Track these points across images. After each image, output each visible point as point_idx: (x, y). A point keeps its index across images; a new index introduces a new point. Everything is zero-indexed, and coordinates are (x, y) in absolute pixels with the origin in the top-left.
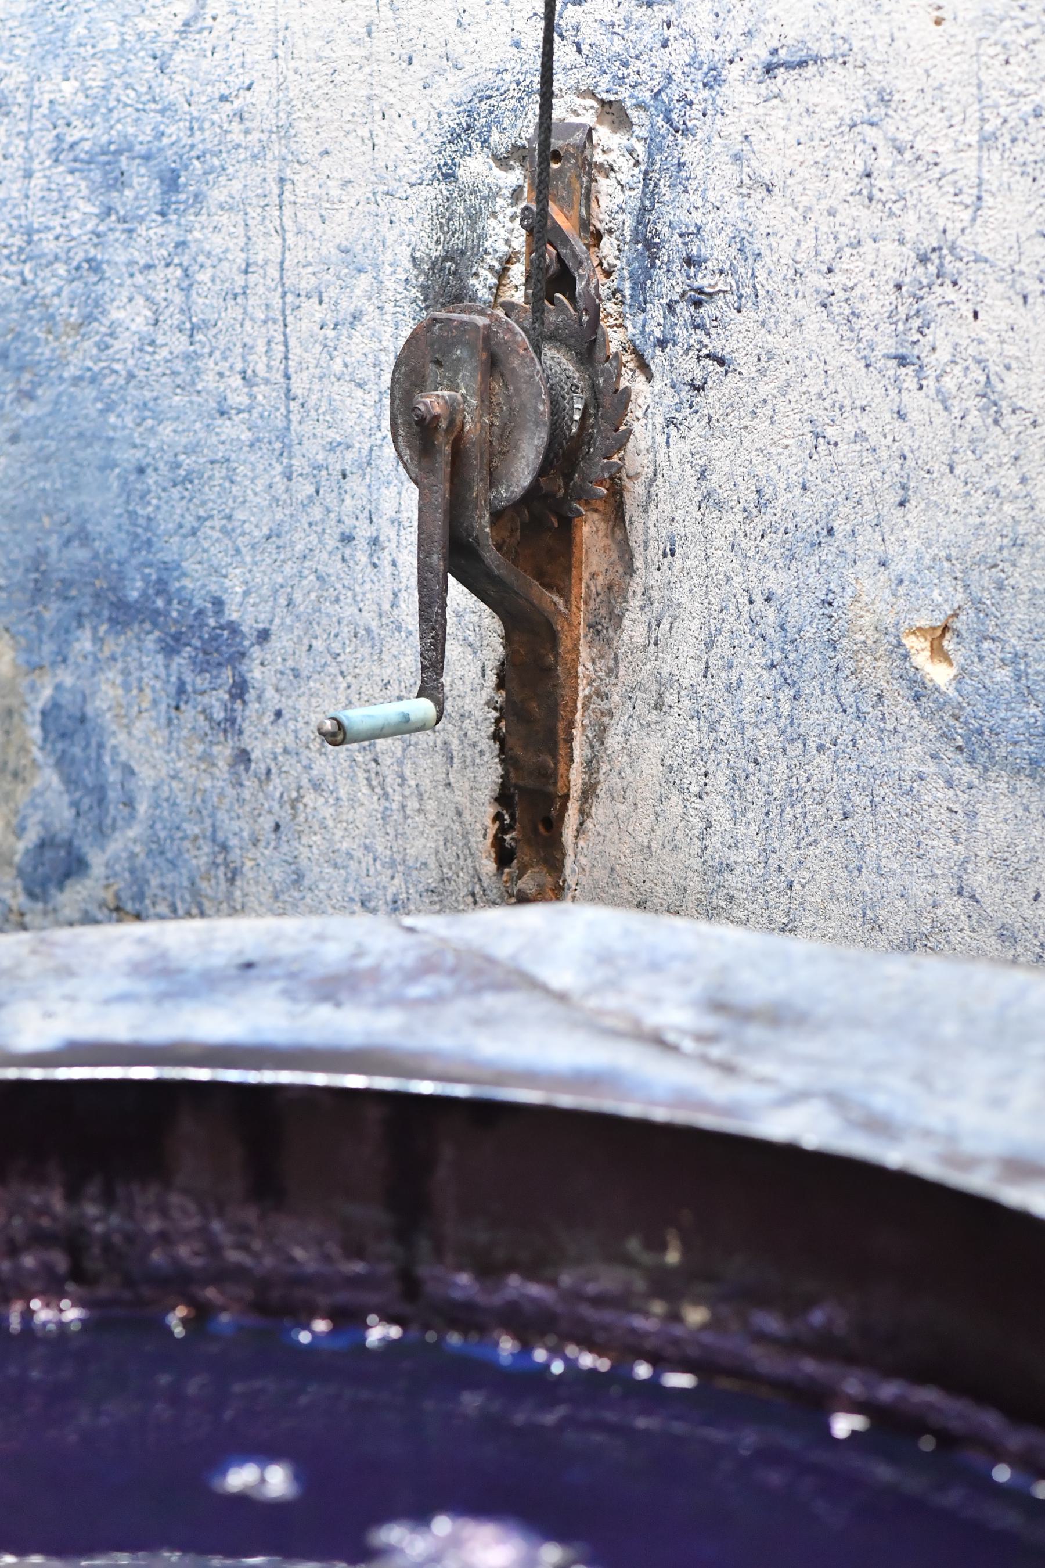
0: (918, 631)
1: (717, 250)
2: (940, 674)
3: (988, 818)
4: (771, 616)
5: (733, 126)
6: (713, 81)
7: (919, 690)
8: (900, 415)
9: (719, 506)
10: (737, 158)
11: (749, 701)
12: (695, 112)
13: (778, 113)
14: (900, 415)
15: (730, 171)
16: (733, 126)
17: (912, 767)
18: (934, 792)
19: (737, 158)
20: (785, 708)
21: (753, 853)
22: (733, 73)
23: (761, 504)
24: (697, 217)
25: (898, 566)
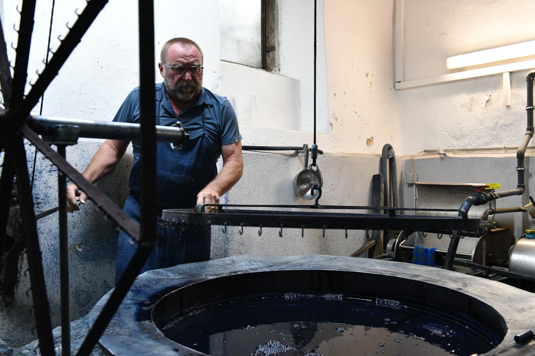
0: (77, 245)
1: (42, 196)
2: (80, 250)
3: (87, 268)
4: (52, 247)
5: (44, 179)
6: (41, 172)
7: (77, 252)
8: (73, 217)
9: (42, 233)
10: (45, 183)
11: (48, 261)
12: (37, 177)
13: (52, 177)
14: (73, 217)
15: (44, 185)
16: (44, 179)
17: (76, 263)
18: (80, 266)
19: (45, 183)
20: (55, 260)
21: (50, 283)
22: (44, 171)
23: (50, 231)
24: (38, 192)
25: (74, 237)
